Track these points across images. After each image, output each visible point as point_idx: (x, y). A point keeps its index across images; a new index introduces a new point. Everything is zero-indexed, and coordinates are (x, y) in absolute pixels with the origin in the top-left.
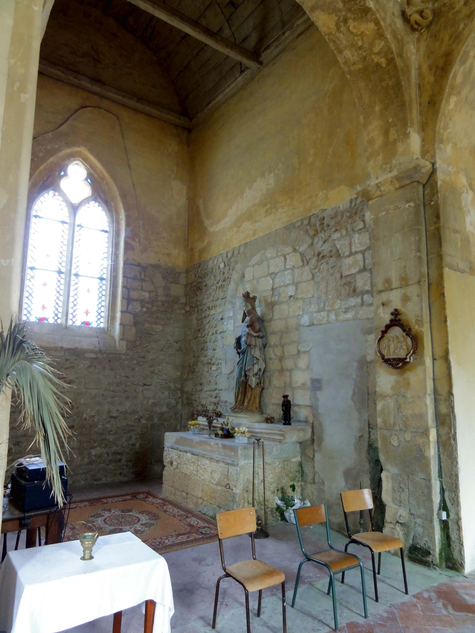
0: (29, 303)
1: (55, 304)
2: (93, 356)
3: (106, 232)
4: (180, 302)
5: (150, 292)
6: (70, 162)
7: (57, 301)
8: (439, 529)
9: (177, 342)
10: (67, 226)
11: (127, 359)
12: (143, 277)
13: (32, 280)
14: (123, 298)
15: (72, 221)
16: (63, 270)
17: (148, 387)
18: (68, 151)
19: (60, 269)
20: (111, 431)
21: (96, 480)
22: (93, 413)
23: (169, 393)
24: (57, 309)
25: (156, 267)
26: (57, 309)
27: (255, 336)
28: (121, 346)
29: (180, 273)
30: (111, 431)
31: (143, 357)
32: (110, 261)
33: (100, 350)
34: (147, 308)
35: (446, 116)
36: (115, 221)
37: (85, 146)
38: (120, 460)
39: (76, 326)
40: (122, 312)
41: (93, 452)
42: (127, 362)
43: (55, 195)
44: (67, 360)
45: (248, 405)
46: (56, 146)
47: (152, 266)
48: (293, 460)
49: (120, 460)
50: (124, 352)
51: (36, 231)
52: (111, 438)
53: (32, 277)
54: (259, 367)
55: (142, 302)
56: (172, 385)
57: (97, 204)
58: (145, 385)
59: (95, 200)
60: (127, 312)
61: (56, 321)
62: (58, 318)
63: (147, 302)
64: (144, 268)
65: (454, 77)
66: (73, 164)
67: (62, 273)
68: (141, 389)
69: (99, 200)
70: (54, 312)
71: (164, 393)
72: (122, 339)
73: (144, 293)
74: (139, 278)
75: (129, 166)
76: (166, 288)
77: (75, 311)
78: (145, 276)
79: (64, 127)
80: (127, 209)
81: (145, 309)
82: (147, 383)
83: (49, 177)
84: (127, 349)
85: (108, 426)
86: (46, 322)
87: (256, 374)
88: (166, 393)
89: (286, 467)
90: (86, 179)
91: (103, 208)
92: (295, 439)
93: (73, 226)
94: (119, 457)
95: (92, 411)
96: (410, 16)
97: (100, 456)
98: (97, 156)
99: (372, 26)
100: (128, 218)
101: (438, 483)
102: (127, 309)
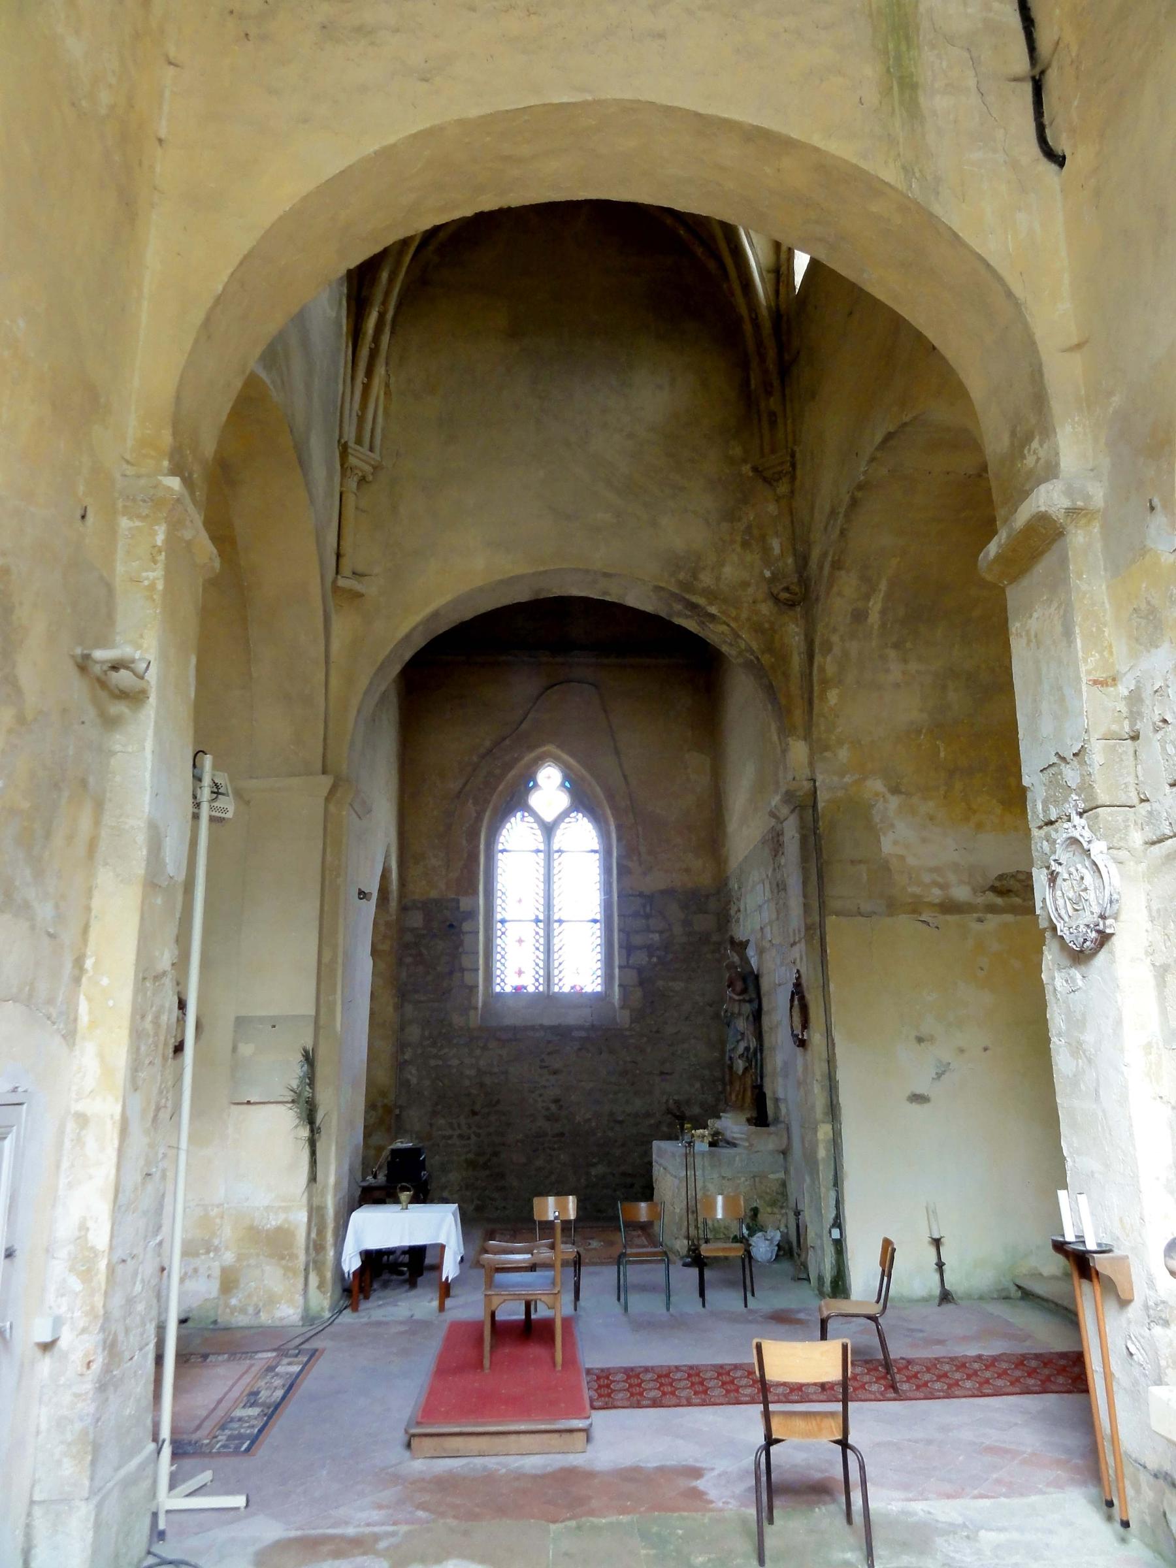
0: (503, 968)
2: (583, 1034)
3: (595, 852)
5: (661, 932)
8: (833, 1252)
9: (711, 1006)
10: (541, 855)
12: (648, 909)
13: (503, 937)
14: (620, 947)
15: (547, 848)
16: (541, 917)
18: (533, 755)
19: (537, 916)
20: (616, 1141)
22: (588, 1116)
23: (702, 1087)
24: (537, 973)
25: (669, 892)
27: (740, 1001)
28: (624, 1018)
29: (707, 897)
32: (602, 893)
33: (593, 1026)
34: (658, 957)
36: (604, 835)
38: (632, 1186)
40: (620, 967)
41: (593, 1172)
42: (632, 1041)
44: (549, 1042)
47: (662, 892)
49: (632, 1186)
50: (627, 1026)
51: (504, 871)
53: (503, 933)
55: (650, 949)
57: (580, 815)
58: (662, 1073)
63: (658, 949)
64: (649, 898)
65: (822, 669)
69: (581, 809)
70: (534, 977)
72: (622, 1008)
73: (651, 936)
74: (642, 913)
75: (617, 752)
76: (686, 923)
78: (651, 910)
79: (524, 726)
80: (616, 818)
84: (631, 1023)
85: (610, 1134)
87: (743, 1054)
88: (698, 1085)
90: (563, 785)
91: (588, 818)
92: (771, 1146)
93: (549, 855)
100: (619, 828)
101: (833, 1194)
102: (628, 963)
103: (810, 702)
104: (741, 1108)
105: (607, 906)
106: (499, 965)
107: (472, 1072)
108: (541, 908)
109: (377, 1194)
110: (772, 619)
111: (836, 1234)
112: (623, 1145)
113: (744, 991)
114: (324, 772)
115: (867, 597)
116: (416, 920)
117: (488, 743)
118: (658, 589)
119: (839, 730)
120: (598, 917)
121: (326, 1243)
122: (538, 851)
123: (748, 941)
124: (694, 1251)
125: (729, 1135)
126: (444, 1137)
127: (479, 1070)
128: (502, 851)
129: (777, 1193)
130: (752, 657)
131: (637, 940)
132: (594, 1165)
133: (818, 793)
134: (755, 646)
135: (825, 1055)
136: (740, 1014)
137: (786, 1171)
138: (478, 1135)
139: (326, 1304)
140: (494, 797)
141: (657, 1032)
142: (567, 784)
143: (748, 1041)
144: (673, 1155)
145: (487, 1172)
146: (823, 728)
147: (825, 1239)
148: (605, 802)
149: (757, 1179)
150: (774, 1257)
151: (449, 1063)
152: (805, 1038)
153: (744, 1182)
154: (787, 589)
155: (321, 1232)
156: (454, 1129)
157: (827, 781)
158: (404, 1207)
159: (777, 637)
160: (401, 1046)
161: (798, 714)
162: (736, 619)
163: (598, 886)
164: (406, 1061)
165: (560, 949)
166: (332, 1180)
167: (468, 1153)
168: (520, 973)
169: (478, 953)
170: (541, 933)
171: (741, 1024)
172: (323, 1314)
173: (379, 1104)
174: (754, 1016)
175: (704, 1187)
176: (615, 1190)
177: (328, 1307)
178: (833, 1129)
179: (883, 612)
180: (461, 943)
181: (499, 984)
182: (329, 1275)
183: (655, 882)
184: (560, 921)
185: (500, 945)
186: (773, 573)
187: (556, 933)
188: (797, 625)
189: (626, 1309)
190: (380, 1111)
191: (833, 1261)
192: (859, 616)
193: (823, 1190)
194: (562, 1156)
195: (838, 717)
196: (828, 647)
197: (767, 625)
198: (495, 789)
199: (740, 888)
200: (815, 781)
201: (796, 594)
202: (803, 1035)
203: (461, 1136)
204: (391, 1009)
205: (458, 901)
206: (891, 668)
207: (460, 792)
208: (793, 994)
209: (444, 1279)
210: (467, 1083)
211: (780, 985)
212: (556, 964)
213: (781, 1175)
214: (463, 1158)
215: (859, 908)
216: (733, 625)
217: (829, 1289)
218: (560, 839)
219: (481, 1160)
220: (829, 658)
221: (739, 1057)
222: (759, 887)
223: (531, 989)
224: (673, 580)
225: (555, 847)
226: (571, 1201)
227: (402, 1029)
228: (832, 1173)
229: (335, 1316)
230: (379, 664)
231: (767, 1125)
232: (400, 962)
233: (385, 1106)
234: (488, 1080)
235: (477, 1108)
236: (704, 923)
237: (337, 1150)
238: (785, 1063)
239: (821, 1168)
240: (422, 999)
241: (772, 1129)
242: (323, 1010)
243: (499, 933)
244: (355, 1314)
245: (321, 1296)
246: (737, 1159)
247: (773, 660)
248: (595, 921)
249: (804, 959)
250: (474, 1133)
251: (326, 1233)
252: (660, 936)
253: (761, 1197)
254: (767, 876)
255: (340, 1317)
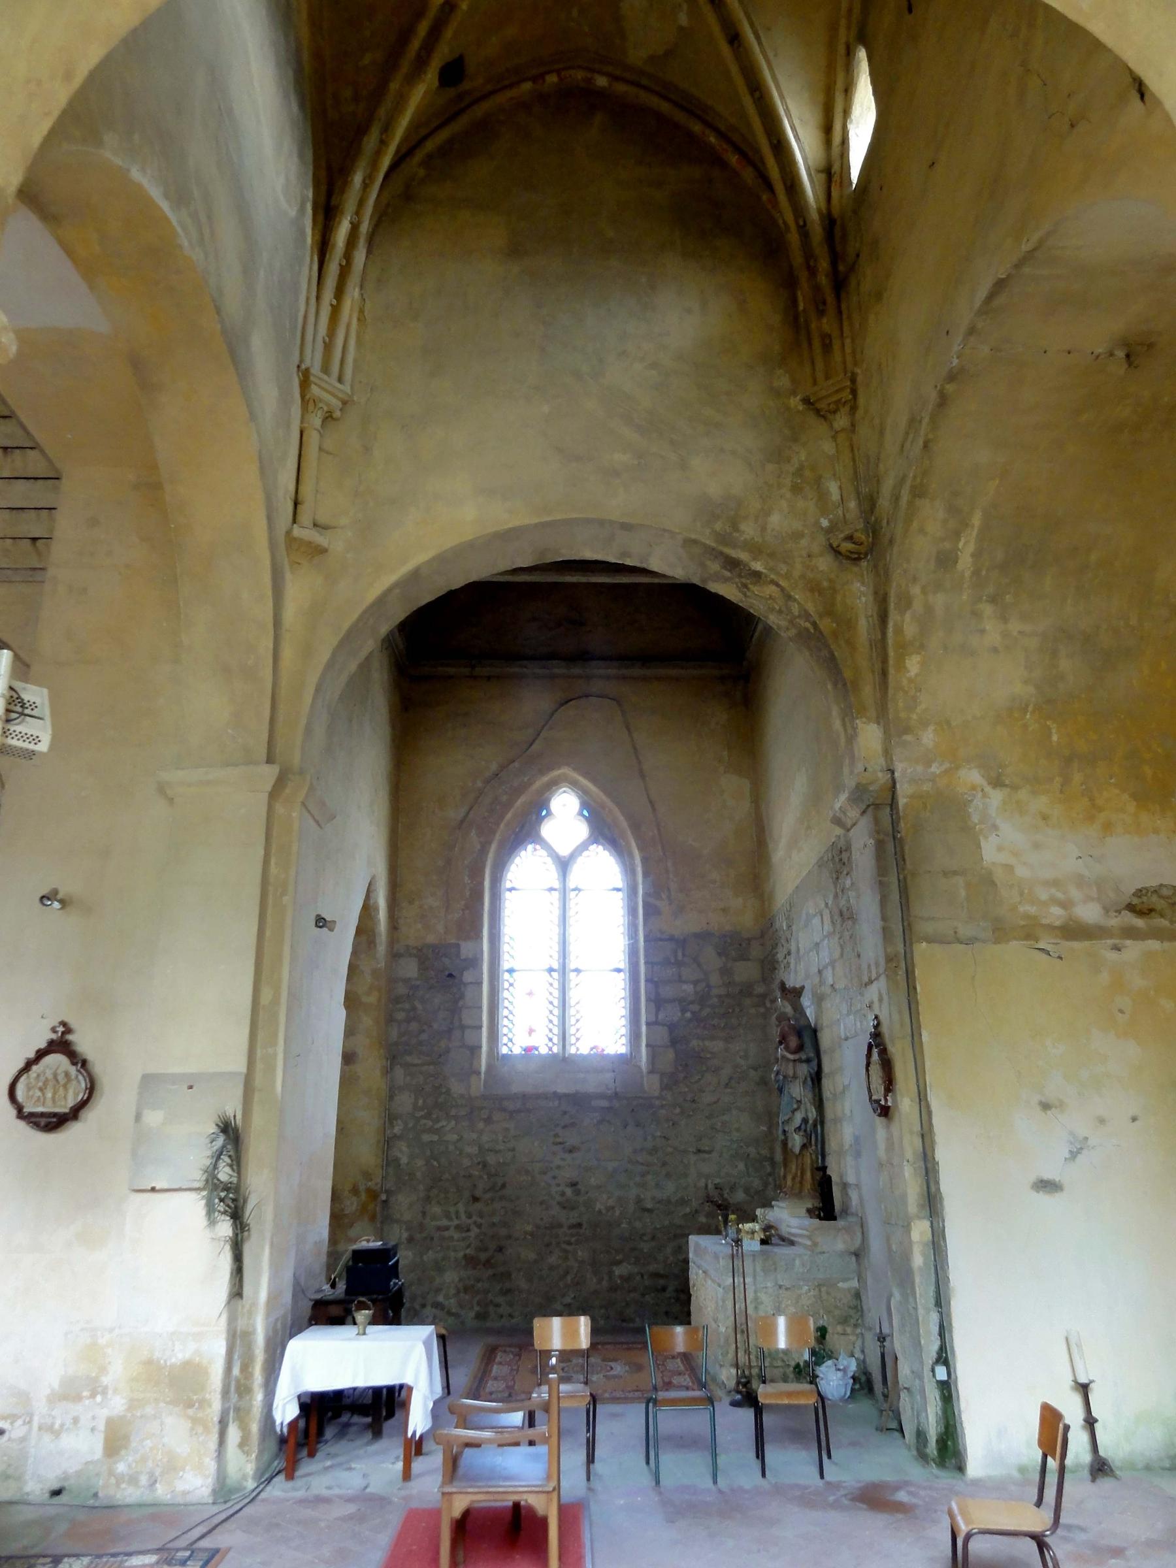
0: (510, 1026)
1: (547, 1022)
2: (604, 1103)
3: (618, 890)
4: (755, 992)
5: (695, 983)
6: (552, 794)
7: (551, 1017)
9: (755, 1069)
11: (662, 1106)
13: (511, 989)
14: (648, 1000)
15: (562, 886)
17: (707, 1156)
18: (545, 779)
21: (623, 1321)
22: (611, 1203)
23: (746, 1165)
25: (703, 936)
26: (551, 1030)
27: (795, 1061)
28: (652, 1085)
29: (749, 940)
30: (644, 1235)
31: (694, 1101)
32: (627, 938)
33: (616, 1094)
34: (693, 1013)
35: (906, 689)
37: (568, 765)
38: (664, 1289)
39: (581, 1055)
40: (648, 1024)
41: (618, 1271)
42: (663, 1112)
43: (535, 850)
44: (565, 1113)
45: (793, 1185)
46: (526, 779)
47: (697, 936)
48: (840, 1285)
49: (664, 1289)
50: (656, 1094)
52: (646, 1247)
53: (511, 985)
54: (803, 1115)
55: (683, 1003)
56: (752, 1150)
57: (601, 847)
58: (699, 1151)
59: (596, 841)
60: (656, 1023)
61: (550, 1049)
62: (554, 1044)
63: (692, 1002)
65: (899, 631)
66: (557, 794)
67: (554, 970)
68: (693, 1158)
69: (601, 840)
71: (736, 1166)
72: (651, 1072)
73: (685, 987)
75: (642, 775)
76: (725, 971)
77: (578, 1030)
78: (684, 955)
79: (536, 747)
80: (641, 849)
81: (688, 1015)
82: (702, 1148)
83: (523, 826)
84: (662, 1089)
85: (638, 1224)
86: (536, 1052)
87: (799, 1128)
88: (741, 1166)
89: (824, 1296)
91: (610, 852)
92: (840, 1246)
94: (662, 1282)
95: (609, 1198)
96: (838, 546)
97: (627, 1279)
98: (586, 775)
99: (773, 588)
100: (645, 861)
101: (934, 1317)
103: (884, 673)
104: (798, 1195)
105: (633, 953)
106: (505, 1022)
107: (474, 1150)
108: (556, 956)
109: (335, 1311)
110: (832, 576)
111: (941, 1373)
112: (653, 1238)
113: (800, 1048)
114: (270, 760)
115: (957, 535)
116: (410, 969)
117: (494, 767)
118: (689, 543)
119: (923, 706)
120: (622, 966)
121: (253, 1383)
122: (551, 889)
123: (803, 988)
124: (745, 1385)
125: (784, 1230)
126: (439, 1229)
127: (480, 1148)
128: (510, 890)
129: (850, 1307)
130: (808, 625)
131: (668, 991)
132: (619, 1263)
133: (898, 786)
134: (810, 607)
135: (917, 1128)
136: (795, 1077)
137: (860, 1278)
138: (479, 1226)
139: (250, 1468)
140: (502, 826)
141: (694, 1101)
142: (586, 813)
143: (806, 1111)
144: (716, 1257)
145: (490, 1272)
146: (901, 704)
147: (926, 1380)
148: (629, 833)
149: (824, 1289)
150: (848, 1394)
151: (445, 1138)
152: (889, 1104)
153: (806, 1293)
154: (850, 538)
155: (246, 1368)
156: (450, 1219)
157: (909, 771)
158: (361, 1331)
159: (839, 598)
160: (391, 1117)
161: (868, 691)
162: (788, 576)
163: (622, 929)
164: (395, 1136)
165: (578, 1003)
166: (263, 1295)
167: (468, 1246)
168: (531, 1031)
169: (480, 1008)
170: (556, 984)
171: (797, 1090)
172: (245, 1483)
173: (362, 1188)
174: (812, 1080)
175: (756, 1299)
176: (643, 1295)
177: (251, 1473)
178: (932, 1227)
179: (977, 555)
180: (462, 997)
181: (506, 1045)
182: (255, 1428)
183: (689, 924)
184: (578, 971)
185: (507, 999)
186: (830, 521)
187: (572, 985)
188: (863, 584)
189: (658, 1482)
190: (363, 1196)
191: (940, 1413)
192: (946, 560)
193: (921, 1311)
194: (580, 1253)
195: (920, 691)
196: (906, 602)
197: (825, 584)
198: (502, 817)
199: (789, 927)
200: (893, 772)
201: (861, 544)
202: (886, 1100)
203: (457, 1227)
204: (378, 1073)
205: (458, 946)
206: (987, 628)
207: (462, 822)
208: (870, 1047)
209: (409, 1435)
210: (466, 1162)
211: (846, 1039)
212: (573, 1021)
213: (854, 1283)
214: (461, 1254)
215: (956, 932)
216: (782, 583)
217: (935, 1452)
218: (576, 875)
219: (483, 1256)
220: (908, 616)
221: (795, 1131)
222: (816, 921)
223: (544, 1051)
224: (708, 531)
225: (572, 882)
226: (583, 1323)
227: (391, 1097)
228: (932, 1288)
229: (262, 1486)
230: (343, 632)
231: (835, 1219)
232: (390, 1020)
233: (369, 1191)
234: (491, 1159)
235: (478, 1193)
236: (746, 971)
237: (271, 1254)
238: (857, 1139)
239: (917, 1280)
240: (416, 1061)
241: (840, 1223)
242: (259, 1066)
243: (506, 985)
244: (290, 1484)
245: (243, 1458)
246: (797, 1262)
247: (834, 625)
248: (619, 970)
249: (885, 997)
250: (475, 1223)
251: (253, 1368)
252: (694, 988)
253: (829, 1312)
254: (827, 904)
255: (269, 1488)
